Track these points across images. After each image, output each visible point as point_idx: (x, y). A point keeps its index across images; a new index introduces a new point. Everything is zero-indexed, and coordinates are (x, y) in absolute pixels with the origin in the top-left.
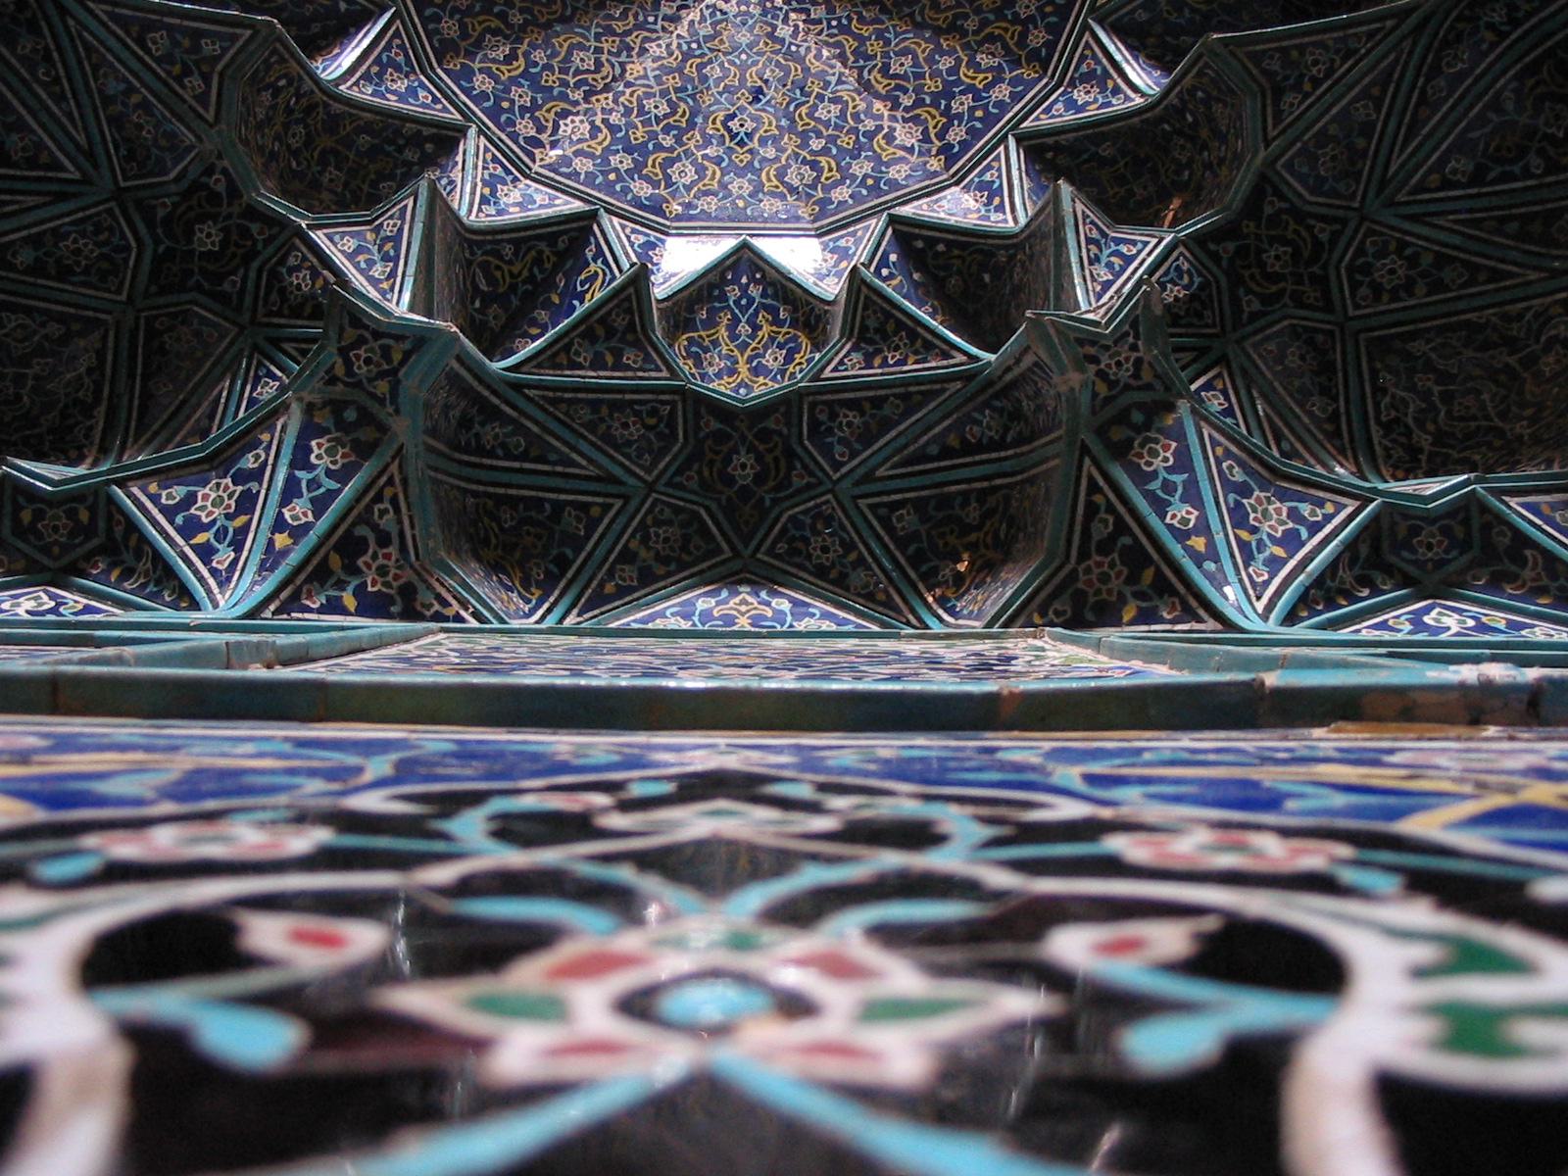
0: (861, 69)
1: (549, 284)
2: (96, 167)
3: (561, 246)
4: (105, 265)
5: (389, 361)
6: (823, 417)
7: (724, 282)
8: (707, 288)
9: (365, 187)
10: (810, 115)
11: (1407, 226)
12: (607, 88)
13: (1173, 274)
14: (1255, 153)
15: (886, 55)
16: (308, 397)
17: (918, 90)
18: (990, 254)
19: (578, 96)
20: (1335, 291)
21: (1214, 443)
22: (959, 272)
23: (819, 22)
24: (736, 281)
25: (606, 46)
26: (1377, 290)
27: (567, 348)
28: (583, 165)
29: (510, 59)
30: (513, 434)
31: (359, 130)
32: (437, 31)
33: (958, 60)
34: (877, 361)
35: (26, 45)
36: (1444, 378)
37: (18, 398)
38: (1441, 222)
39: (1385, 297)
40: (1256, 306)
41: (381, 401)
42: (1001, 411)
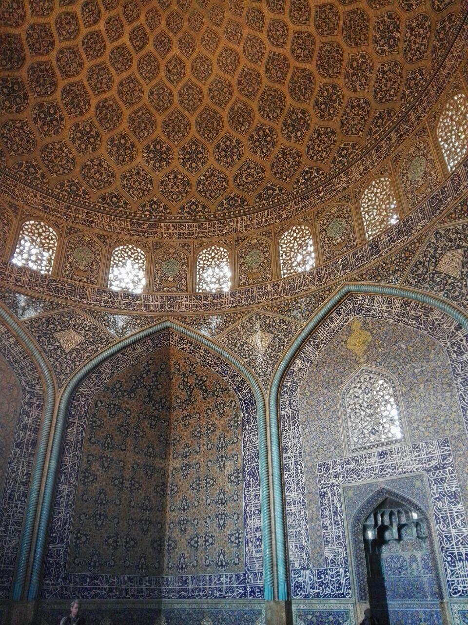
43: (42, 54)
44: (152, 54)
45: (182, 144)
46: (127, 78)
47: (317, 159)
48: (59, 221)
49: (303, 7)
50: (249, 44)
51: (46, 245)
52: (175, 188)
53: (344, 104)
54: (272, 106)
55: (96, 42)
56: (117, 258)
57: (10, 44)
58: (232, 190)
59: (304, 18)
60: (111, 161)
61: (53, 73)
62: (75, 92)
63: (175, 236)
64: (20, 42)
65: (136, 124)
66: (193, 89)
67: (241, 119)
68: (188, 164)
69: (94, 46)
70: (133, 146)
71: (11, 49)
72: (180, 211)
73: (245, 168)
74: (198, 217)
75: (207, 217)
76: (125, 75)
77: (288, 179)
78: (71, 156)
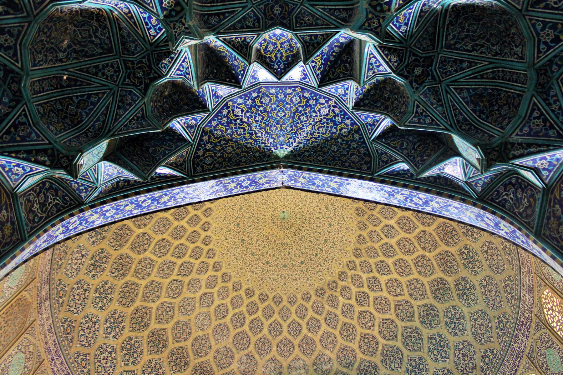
0: (251, 130)
1: (330, 67)
2: (446, 89)
3: (327, 78)
4: (445, 63)
5: (368, 23)
6: (256, 24)
7: (284, 69)
8: (289, 65)
9: (378, 92)
10: (264, 117)
11: (106, 83)
12: (316, 123)
13: (166, 67)
14: (147, 101)
15: (245, 134)
16: (389, 13)
17: (236, 124)
18: (215, 77)
19: (324, 120)
20: (123, 66)
21: (152, 7)
22: (223, 73)
23: (263, 143)
24: (281, 69)
25: (317, 134)
26: (112, 66)
27: (324, 39)
28: (322, 101)
29: (341, 129)
30: (338, 15)
31: (380, 107)
32: (360, 135)
33: (226, 132)
34: (243, 39)
35: (461, 118)
36: (92, 42)
37: (468, 26)
38: (98, 85)
39: (110, 64)
40: (144, 60)
41: (371, 12)
42: (209, 24)
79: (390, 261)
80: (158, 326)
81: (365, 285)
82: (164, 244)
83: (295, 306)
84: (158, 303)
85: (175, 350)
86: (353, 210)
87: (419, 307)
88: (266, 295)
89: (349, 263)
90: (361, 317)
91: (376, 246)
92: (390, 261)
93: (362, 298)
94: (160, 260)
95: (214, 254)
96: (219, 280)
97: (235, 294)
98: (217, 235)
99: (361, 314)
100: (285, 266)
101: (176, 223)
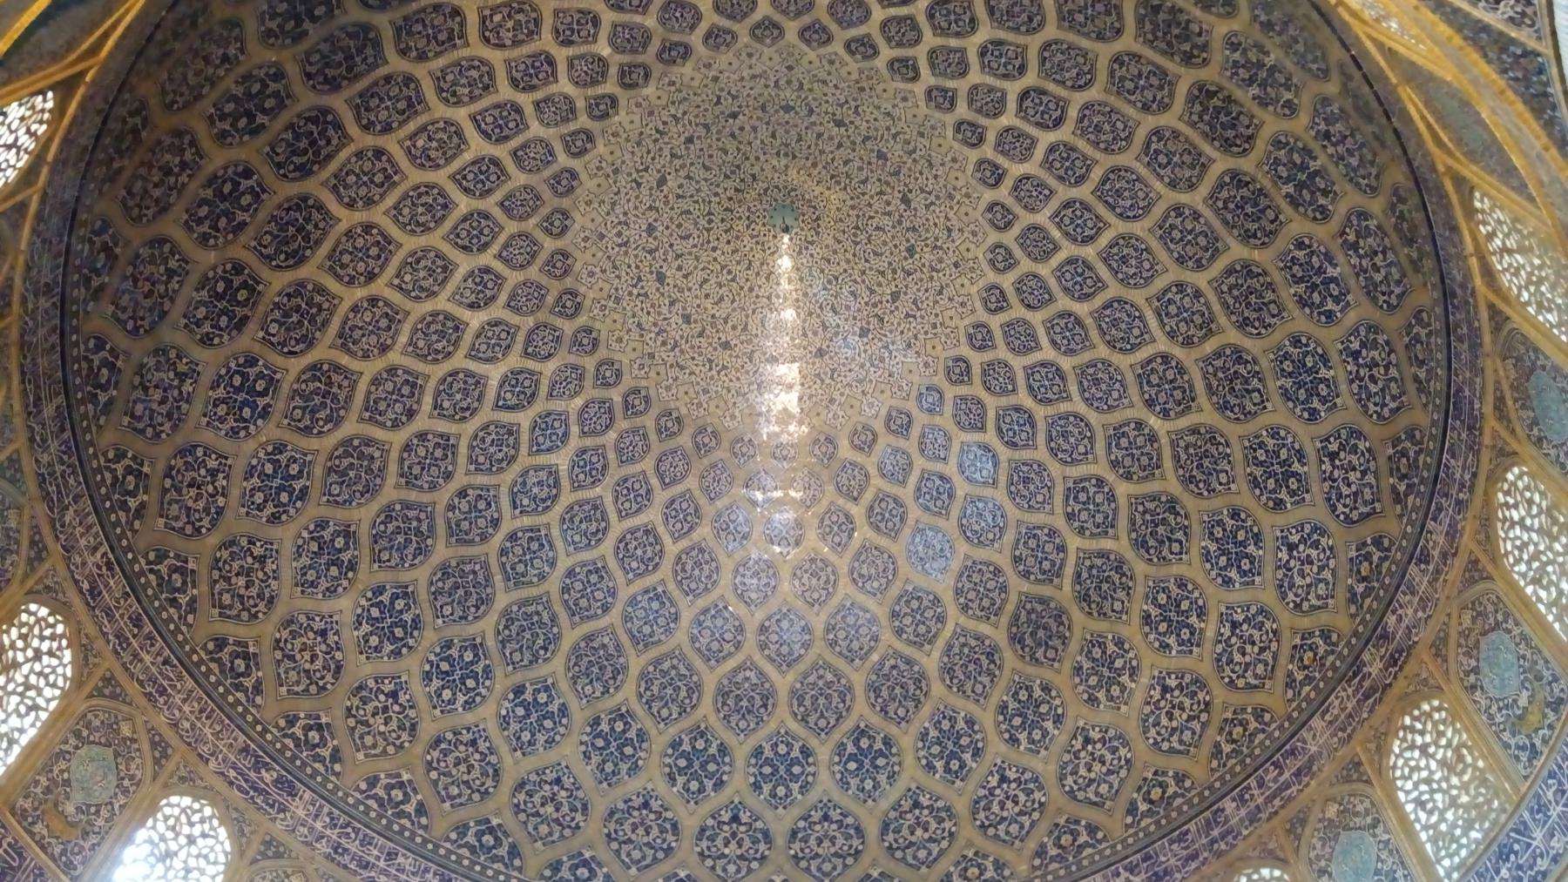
43: (338, 277)
44: (518, 431)
45: (449, 632)
46: (441, 436)
47: (713, 868)
48: (99, 644)
49: (824, 578)
50: (694, 553)
51: (32, 693)
52: (380, 719)
53: (814, 796)
54: (669, 691)
55: (442, 334)
56: (161, 826)
57: (308, 220)
58: (499, 810)
59: (816, 596)
60: (288, 568)
61: (326, 323)
62: (330, 384)
63: (323, 847)
64: (325, 233)
65: (391, 527)
66: (542, 545)
67: (595, 670)
68: (436, 683)
69: (435, 337)
70: (352, 566)
71: (300, 230)
72: (363, 786)
73: (550, 776)
74: (396, 827)
75: (418, 840)
76: (443, 426)
77: (633, 871)
78: (221, 501)
79: (464, 204)
80: (1207, 149)
81: (529, 110)
82: (1114, 331)
83: (757, 16)
84: (1184, 198)
85: (1177, 58)
86: (588, 303)
87: (346, 138)
88: (852, 53)
89: (589, 146)
90: (532, 26)
91: (512, 227)
92: (464, 204)
93: (535, 72)
94: (1138, 296)
95: (991, 208)
96: (991, 137)
97: (950, 84)
98: (970, 255)
99: (531, 33)
100: (787, 109)
101: (1066, 363)
